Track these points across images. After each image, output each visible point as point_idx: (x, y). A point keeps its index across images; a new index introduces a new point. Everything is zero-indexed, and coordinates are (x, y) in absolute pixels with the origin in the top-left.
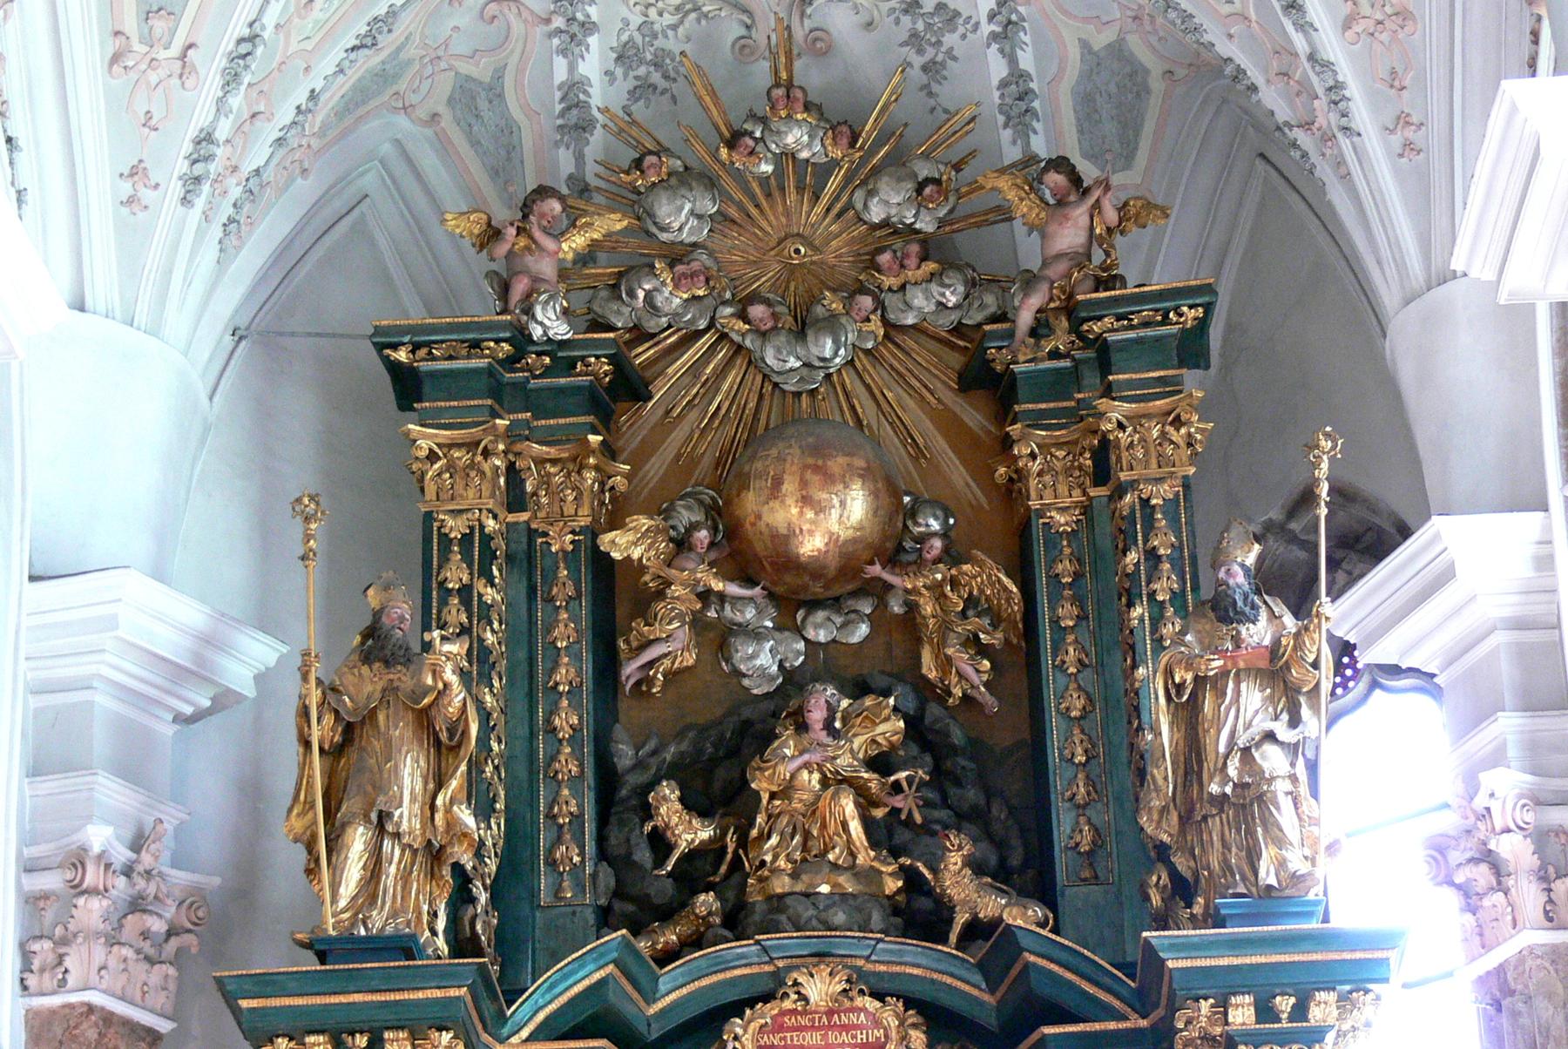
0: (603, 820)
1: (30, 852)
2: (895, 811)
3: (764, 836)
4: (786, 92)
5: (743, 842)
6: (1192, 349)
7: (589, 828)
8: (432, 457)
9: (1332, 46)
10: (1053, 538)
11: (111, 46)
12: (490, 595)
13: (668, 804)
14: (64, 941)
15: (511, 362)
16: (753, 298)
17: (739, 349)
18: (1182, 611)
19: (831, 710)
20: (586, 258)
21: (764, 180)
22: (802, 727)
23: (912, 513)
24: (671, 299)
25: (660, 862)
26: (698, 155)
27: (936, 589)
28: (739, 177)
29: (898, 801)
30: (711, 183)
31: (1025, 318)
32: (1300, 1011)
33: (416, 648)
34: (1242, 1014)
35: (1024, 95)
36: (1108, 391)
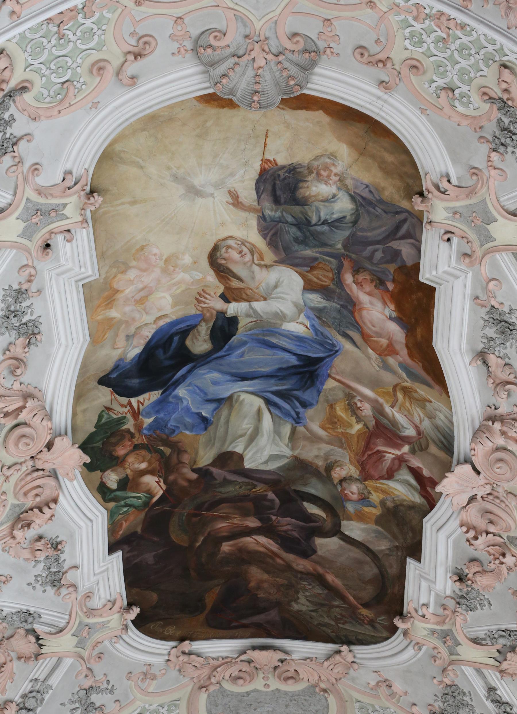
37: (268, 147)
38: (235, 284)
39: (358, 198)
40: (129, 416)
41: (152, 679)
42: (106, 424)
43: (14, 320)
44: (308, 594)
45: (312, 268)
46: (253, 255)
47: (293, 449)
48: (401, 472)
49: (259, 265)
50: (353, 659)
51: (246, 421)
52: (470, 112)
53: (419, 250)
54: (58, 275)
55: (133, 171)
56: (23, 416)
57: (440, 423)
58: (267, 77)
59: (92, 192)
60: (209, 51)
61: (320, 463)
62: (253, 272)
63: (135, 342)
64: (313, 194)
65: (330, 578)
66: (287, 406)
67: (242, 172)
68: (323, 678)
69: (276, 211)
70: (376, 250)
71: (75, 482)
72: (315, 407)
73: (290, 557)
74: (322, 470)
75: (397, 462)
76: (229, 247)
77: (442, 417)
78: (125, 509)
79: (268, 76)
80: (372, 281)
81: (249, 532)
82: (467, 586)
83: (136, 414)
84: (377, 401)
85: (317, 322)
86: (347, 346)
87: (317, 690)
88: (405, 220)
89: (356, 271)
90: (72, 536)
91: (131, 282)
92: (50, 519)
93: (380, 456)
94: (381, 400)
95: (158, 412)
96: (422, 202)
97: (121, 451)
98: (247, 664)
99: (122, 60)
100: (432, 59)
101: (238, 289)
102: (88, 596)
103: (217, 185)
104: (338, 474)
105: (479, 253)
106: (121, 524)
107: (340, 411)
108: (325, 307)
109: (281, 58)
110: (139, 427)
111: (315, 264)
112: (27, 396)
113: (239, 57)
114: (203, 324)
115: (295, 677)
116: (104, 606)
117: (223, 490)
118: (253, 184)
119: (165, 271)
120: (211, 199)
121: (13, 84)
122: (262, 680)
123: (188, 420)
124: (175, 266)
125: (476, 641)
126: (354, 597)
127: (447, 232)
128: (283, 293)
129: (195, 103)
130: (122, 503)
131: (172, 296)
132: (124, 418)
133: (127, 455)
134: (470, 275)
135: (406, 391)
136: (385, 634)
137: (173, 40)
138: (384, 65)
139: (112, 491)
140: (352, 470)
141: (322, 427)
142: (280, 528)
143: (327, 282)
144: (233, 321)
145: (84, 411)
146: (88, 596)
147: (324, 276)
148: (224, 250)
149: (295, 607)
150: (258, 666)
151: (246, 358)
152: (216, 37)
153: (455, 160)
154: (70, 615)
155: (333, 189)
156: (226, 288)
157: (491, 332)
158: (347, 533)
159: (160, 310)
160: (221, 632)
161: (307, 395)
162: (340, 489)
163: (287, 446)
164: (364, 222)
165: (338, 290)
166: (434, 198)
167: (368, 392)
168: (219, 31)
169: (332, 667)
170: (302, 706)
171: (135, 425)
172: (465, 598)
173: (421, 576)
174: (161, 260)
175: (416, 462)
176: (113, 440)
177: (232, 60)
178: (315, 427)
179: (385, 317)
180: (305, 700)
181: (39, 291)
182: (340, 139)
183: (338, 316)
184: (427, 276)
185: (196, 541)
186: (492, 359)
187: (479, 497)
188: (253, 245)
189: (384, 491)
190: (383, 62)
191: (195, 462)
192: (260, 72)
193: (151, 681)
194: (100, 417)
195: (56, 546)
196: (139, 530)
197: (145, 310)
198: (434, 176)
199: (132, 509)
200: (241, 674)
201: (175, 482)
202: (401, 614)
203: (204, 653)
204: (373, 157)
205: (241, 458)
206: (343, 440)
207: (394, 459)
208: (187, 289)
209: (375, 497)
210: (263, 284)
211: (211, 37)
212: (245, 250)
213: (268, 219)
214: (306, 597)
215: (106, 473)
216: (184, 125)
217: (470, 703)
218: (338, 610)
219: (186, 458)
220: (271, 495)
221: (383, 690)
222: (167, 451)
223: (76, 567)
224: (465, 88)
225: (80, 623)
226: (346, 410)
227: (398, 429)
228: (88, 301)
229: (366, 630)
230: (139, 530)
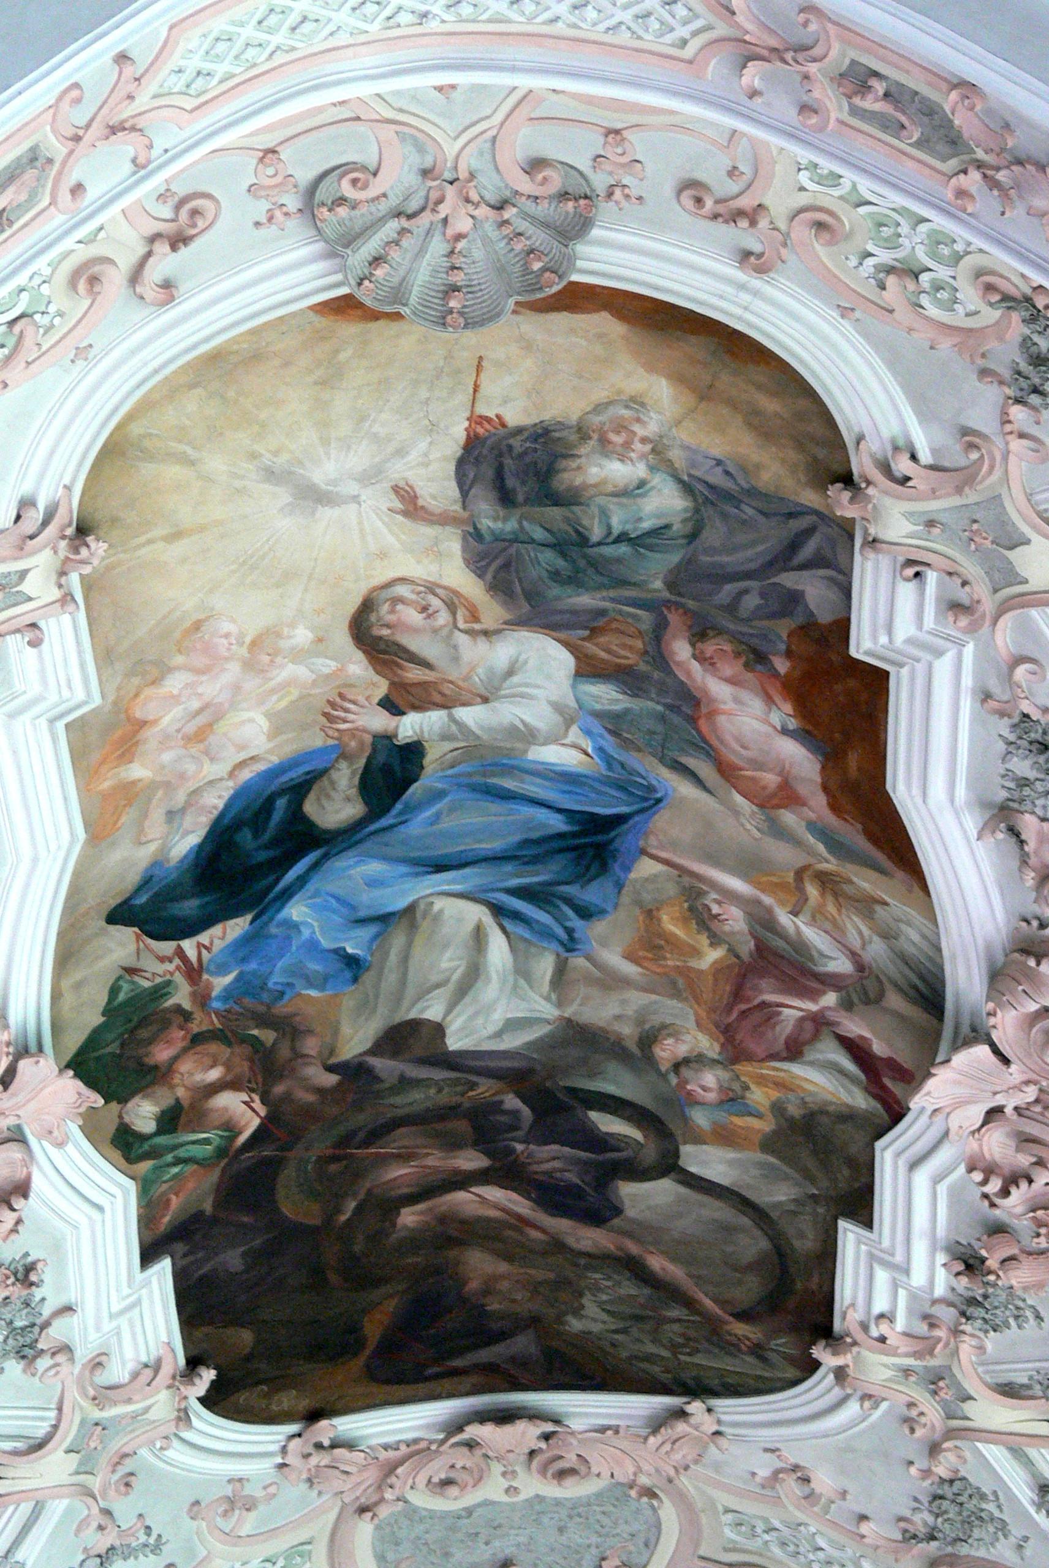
37: (486, 387)
38: (413, 674)
39: (700, 487)
40: (179, 978)
41: (248, 1510)
42: (128, 1002)
44: (604, 1297)
45: (595, 632)
46: (454, 614)
47: (560, 1004)
48: (819, 1045)
49: (466, 632)
50: (715, 1428)
51: (448, 954)
52: (957, 318)
53: (846, 592)
54: (11, 716)
55: (174, 472)
57: (912, 950)
58: (476, 253)
59: (83, 531)
60: (342, 211)
61: (627, 1031)
62: (455, 647)
63: (188, 821)
64: (592, 480)
65: (656, 1263)
66: (541, 916)
67: (423, 446)
68: (646, 1467)
69: (505, 520)
70: (746, 591)
71: (70, 1148)
72: (609, 918)
73: (562, 1225)
74: (632, 1046)
75: (809, 1026)
76: (400, 600)
77: (915, 936)
78: (175, 1170)
79: (478, 254)
80: (738, 655)
81: (462, 1181)
82: (987, 1284)
83: (193, 972)
84: (758, 902)
85: (609, 743)
86: (685, 789)
87: (633, 1493)
88: (810, 531)
89: (700, 634)
90: (57, 1247)
91: (175, 699)
92: (14, 1231)
93: (768, 1013)
94: (767, 900)
95: (244, 960)
96: (852, 500)
97: (161, 1054)
98: (465, 1450)
99: (141, 250)
100: (862, 210)
101: (424, 685)
102: (97, 1364)
103: (367, 478)
105: (988, 605)
106: (168, 1201)
107: (670, 924)
108: (627, 711)
109: (509, 213)
110: (202, 999)
111: (601, 622)
113: (410, 217)
114: (343, 765)
116: (135, 1375)
117: (398, 1100)
118: (451, 467)
119: (249, 666)
120: (356, 506)
122: (501, 1479)
124: (274, 654)
125: (1009, 1391)
126: (715, 1300)
127: (910, 563)
128: (527, 685)
129: (311, 314)
130: (169, 1158)
131: (268, 715)
132: (168, 983)
133: (175, 1059)
134: (969, 650)
135: (825, 880)
136: (791, 1373)
137: (257, 197)
138: (753, 223)
139: (143, 1138)
140: (707, 1044)
141: (630, 956)
142: (535, 1168)
143: (631, 658)
144: (413, 752)
145: (78, 986)
146: (97, 1364)
147: (624, 646)
148: (386, 607)
149: (575, 1325)
150: (490, 1454)
151: (446, 824)
152: (354, 182)
153: (925, 416)
154: (60, 1409)
155: (640, 470)
156: (393, 684)
157: (1023, 766)
158: (693, 1169)
159: (242, 748)
160: (400, 1390)
161: (591, 894)
162: (674, 1080)
163: (547, 999)
164: (714, 534)
165: (656, 675)
166: (879, 493)
168: (364, 168)
169: (667, 1447)
170: (597, 1527)
171: (194, 995)
172: (979, 1304)
173: (872, 1257)
174: (241, 644)
175: (854, 1027)
176: (143, 1033)
177: (394, 225)
178: (614, 959)
179: (770, 730)
180: (604, 1513)
182: (651, 368)
183: (659, 728)
184: (867, 644)
185: (339, 1211)
187: (1009, 1110)
188: (455, 592)
189: (779, 1085)
190: (752, 216)
191: (332, 1052)
192: (461, 245)
193: (245, 1513)
194: (114, 991)
196: (208, 1207)
197: (206, 753)
198: (874, 445)
199: (190, 1168)
200: (453, 1474)
201: (287, 1097)
203: (362, 1438)
204: (733, 404)
205: (439, 1030)
206: (681, 983)
207: (802, 1020)
208: (301, 697)
209: (759, 1097)
210: (480, 671)
211: (345, 184)
212: (436, 602)
213: (488, 538)
214: (600, 1304)
215: (130, 1105)
216: (286, 364)
217: (996, 1513)
218: (676, 1327)
219: (311, 1046)
220: (511, 1102)
221: (790, 1486)
222: (268, 1036)
223: (68, 1309)
224: (943, 273)
225: (83, 1423)
226: (685, 921)
227: (811, 959)
228: (77, 756)
229: (746, 1365)
230: (208, 1207)
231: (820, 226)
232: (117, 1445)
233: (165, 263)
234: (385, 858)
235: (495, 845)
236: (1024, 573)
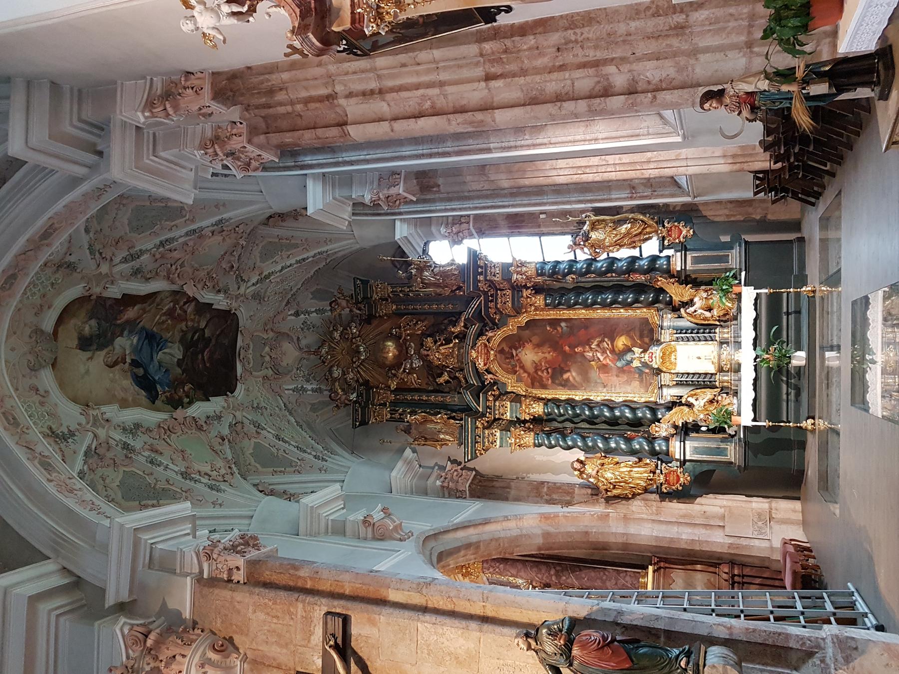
0: (442, 392)
1: (441, 494)
2: (444, 340)
3: (447, 363)
4: (317, 352)
5: (448, 367)
6: (365, 283)
7: (443, 395)
8: (376, 419)
9: (312, 253)
10: (397, 309)
11: (296, 472)
12: (401, 410)
13: (441, 380)
14: (457, 490)
15: (360, 404)
16: (352, 360)
17: (361, 364)
18: (411, 287)
19: (425, 350)
20: (343, 390)
21: (331, 358)
22: (428, 355)
23: (392, 334)
24: (351, 375)
25: (450, 382)
26: (327, 369)
27: (405, 331)
28: (331, 362)
29: (442, 339)
30: (332, 367)
31: (358, 312)
32: (482, 267)
33: (408, 424)
34: (481, 278)
35: (319, 310)
36: (371, 297)
38: (120, 359)
43: (134, 431)
56: (166, 428)
81: (203, 356)
89: (116, 319)
101: (122, 358)
104: (184, 328)
110: (169, 391)
112: (159, 426)
115: (248, 345)
121: (48, 432)
123: (166, 376)
125: (239, 288)
140: (184, 323)
144: (132, 360)
146: (224, 408)
155: (87, 325)
157: (139, 276)
167: (158, 317)
175: (182, 303)
181: (123, 423)
186: (148, 276)
195: (208, 417)
202: (230, 311)
205: (179, 359)
209: (192, 317)
224: (53, 279)
231: (44, 296)
232: (236, 405)
233: (42, 392)
234: (150, 364)
235: (149, 351)
236: (105, 272)
